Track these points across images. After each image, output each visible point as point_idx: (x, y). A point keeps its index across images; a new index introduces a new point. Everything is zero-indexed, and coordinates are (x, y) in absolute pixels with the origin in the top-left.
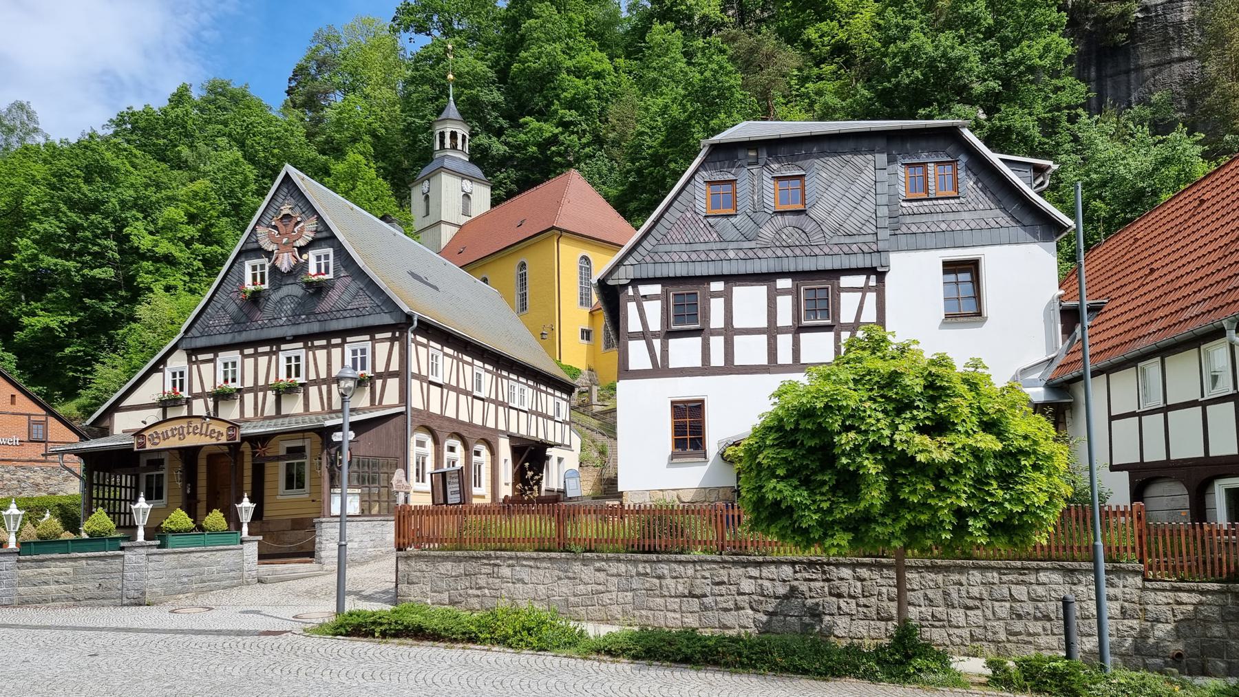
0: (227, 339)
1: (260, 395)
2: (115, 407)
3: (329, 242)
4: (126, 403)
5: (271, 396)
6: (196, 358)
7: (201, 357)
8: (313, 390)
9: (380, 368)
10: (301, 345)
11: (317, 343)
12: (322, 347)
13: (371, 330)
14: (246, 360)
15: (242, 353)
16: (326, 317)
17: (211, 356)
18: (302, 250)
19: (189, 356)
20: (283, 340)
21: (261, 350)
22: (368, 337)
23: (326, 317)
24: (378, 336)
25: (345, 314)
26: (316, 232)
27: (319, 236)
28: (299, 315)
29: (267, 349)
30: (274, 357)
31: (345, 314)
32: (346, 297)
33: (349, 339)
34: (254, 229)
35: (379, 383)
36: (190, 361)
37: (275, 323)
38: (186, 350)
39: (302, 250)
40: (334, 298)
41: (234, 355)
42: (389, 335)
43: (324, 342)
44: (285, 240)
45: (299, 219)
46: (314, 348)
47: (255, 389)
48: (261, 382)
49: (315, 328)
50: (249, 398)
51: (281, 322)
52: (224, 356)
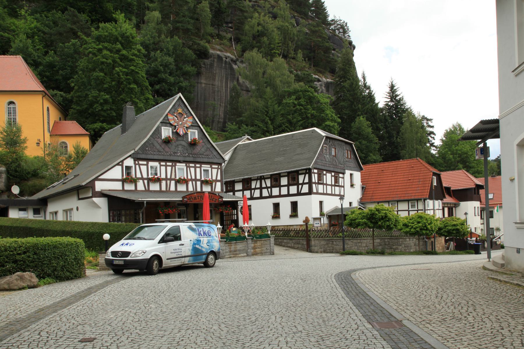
0: (156, 157)
1: (168, 182)
2: (97, 179)
3: (196, 128)
4: (100, 177)
5: (173, 182)
6: (138, 162)
7: (141, 162)
8: (190, 183)
9: (214, 178)
10: (184, 164)
11: (191, 165)
12: (192, 167)
13: (211, 163)
14: (162, 167)
15: (160, 164)
16: (196, 156)
17: (145, 163)
18: (187, 128)
19: (135, 161)
20: (180, 162)
21: (168, 164)
22: (209, 166)
23: (196, 156)
24: (213, 166)
25: (203, 156)
26: (192, 123)
27: (193, 124)
28: (186, 153)
29: (170, 164)
30: (174, 168)
31: (203, 156)
32: (203, 150)
33: (203, 166)
34: (167, 115)
35: (214, 183)
36: (135, 164)
37: (176, 154)
38: (134, 158)
39: (187, 128)
40: (198, 149)
41: (156, 164)
42: (217, 166)
43: (193, 165)
44: (180, 123)
45: (186, 116)
46: (190, 167)
47: (166, 179)
48: (169, 177)
49: (191, 159)
50: (164, 183)
51: (178, 155)
52: (151, 164)
